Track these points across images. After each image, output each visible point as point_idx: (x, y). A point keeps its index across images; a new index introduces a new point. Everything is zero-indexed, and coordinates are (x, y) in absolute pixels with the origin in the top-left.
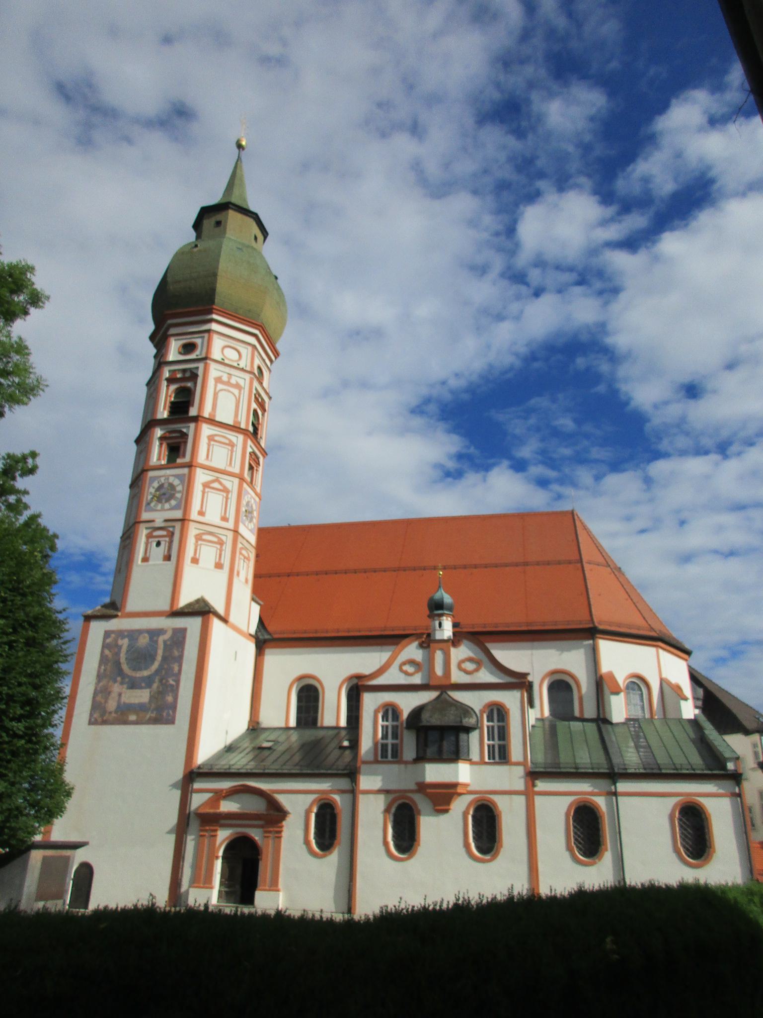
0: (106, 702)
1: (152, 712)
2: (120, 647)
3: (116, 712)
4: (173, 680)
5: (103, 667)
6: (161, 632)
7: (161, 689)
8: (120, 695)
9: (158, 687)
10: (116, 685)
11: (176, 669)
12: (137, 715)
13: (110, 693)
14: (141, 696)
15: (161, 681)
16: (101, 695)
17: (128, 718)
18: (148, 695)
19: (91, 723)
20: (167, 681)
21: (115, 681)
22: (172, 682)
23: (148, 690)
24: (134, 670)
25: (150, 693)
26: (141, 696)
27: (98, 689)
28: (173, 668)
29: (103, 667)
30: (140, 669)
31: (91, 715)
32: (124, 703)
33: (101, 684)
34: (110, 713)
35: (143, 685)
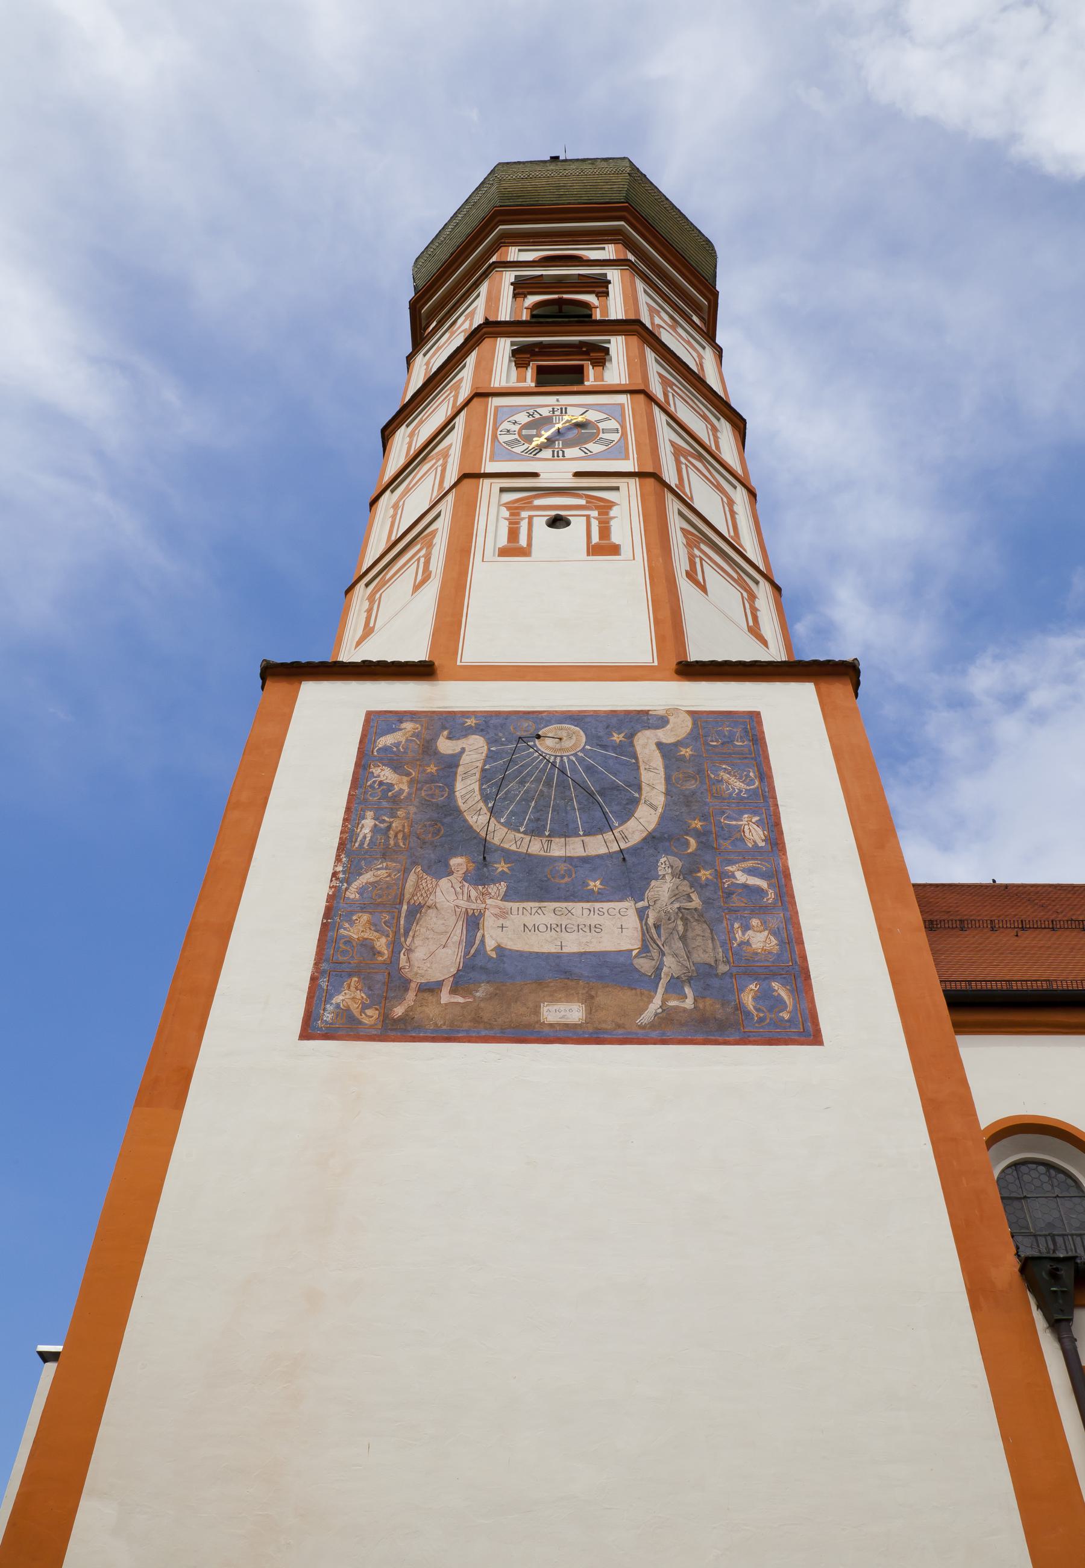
0: (396, 947)
1: (675, 986)
2: (451, 764)
3: (459, 983)
4: (751, 872)
5: (368, 823)
6: (639, 720)
7: (696, 902)
8: (473, 922)
9: (676, 896)
10: (444, 882)
11: (754, 834)
12: (589, 1000)
13: (416, 912)
14: (597, 928)
15: (688, 873)
16: (365, 917)
17: (537, 1011)
18: (632, 921)
19: (310, 1030)
20: (720, 875)
21: (440, 869)
22: (741, 878)
23: (627, 908)
24: (535, 831)
25: (642, 914)
26: (597, 928)
27: (352, 894)
28: (739, 829)
29: (368, 823)
30: (566, 831)
31: (316, 996)
32: (499, 949)
33: (367, 877)
34: (431, 989)
35: (595, 885)
